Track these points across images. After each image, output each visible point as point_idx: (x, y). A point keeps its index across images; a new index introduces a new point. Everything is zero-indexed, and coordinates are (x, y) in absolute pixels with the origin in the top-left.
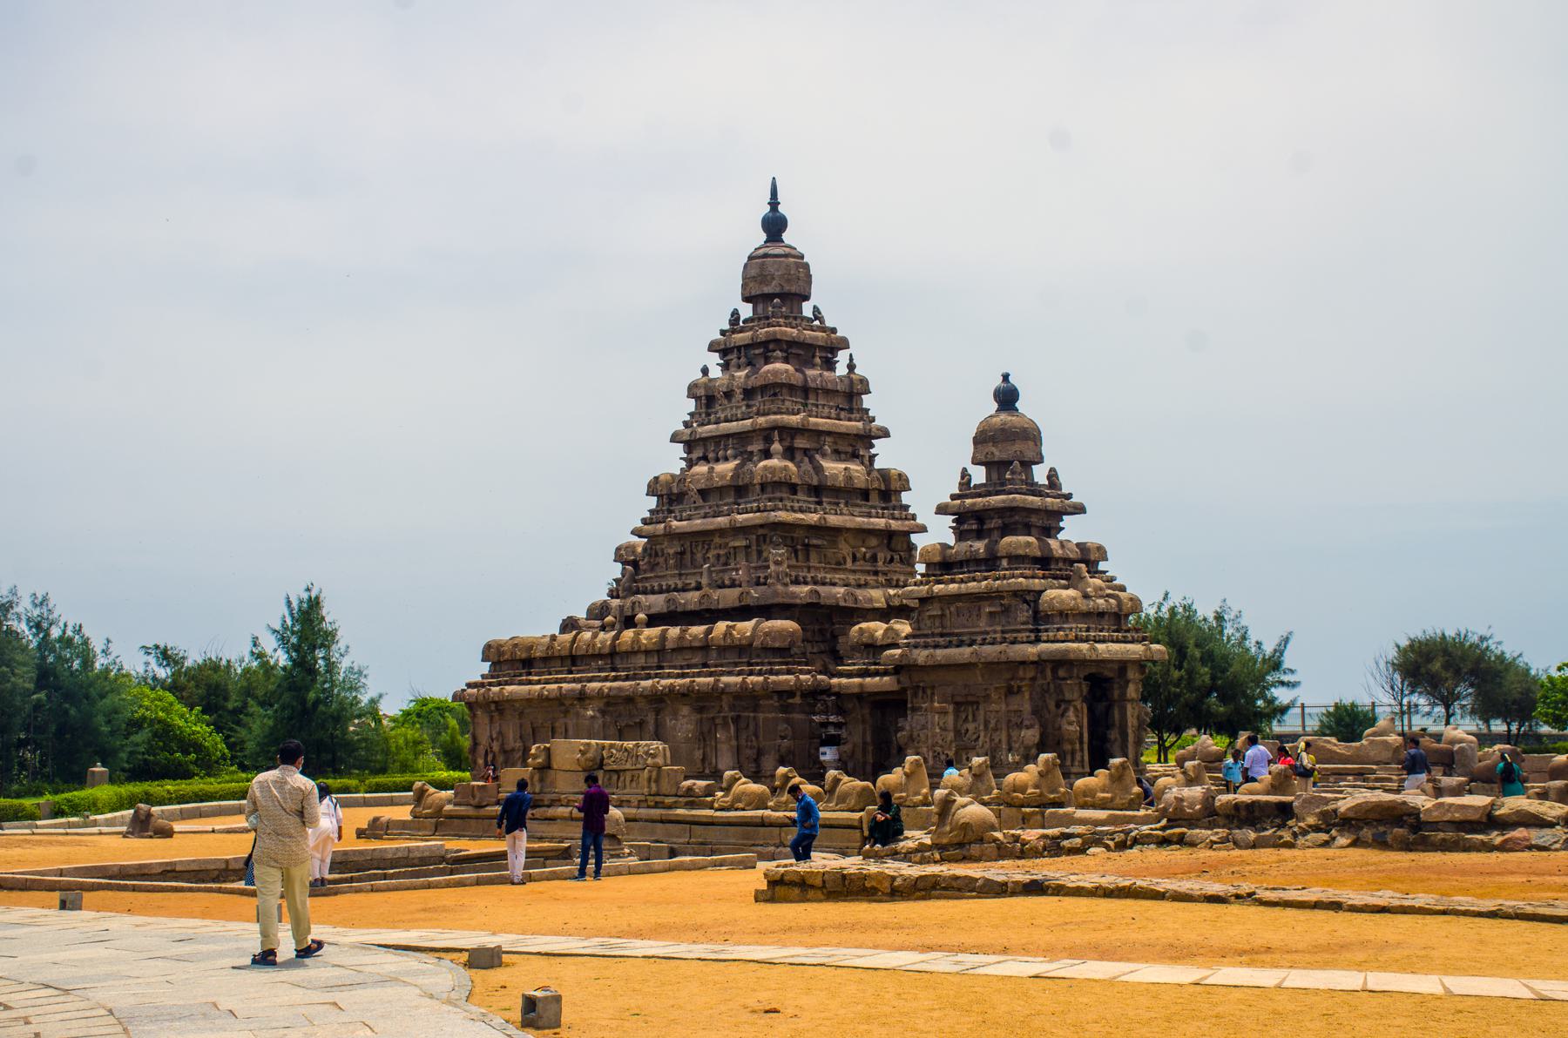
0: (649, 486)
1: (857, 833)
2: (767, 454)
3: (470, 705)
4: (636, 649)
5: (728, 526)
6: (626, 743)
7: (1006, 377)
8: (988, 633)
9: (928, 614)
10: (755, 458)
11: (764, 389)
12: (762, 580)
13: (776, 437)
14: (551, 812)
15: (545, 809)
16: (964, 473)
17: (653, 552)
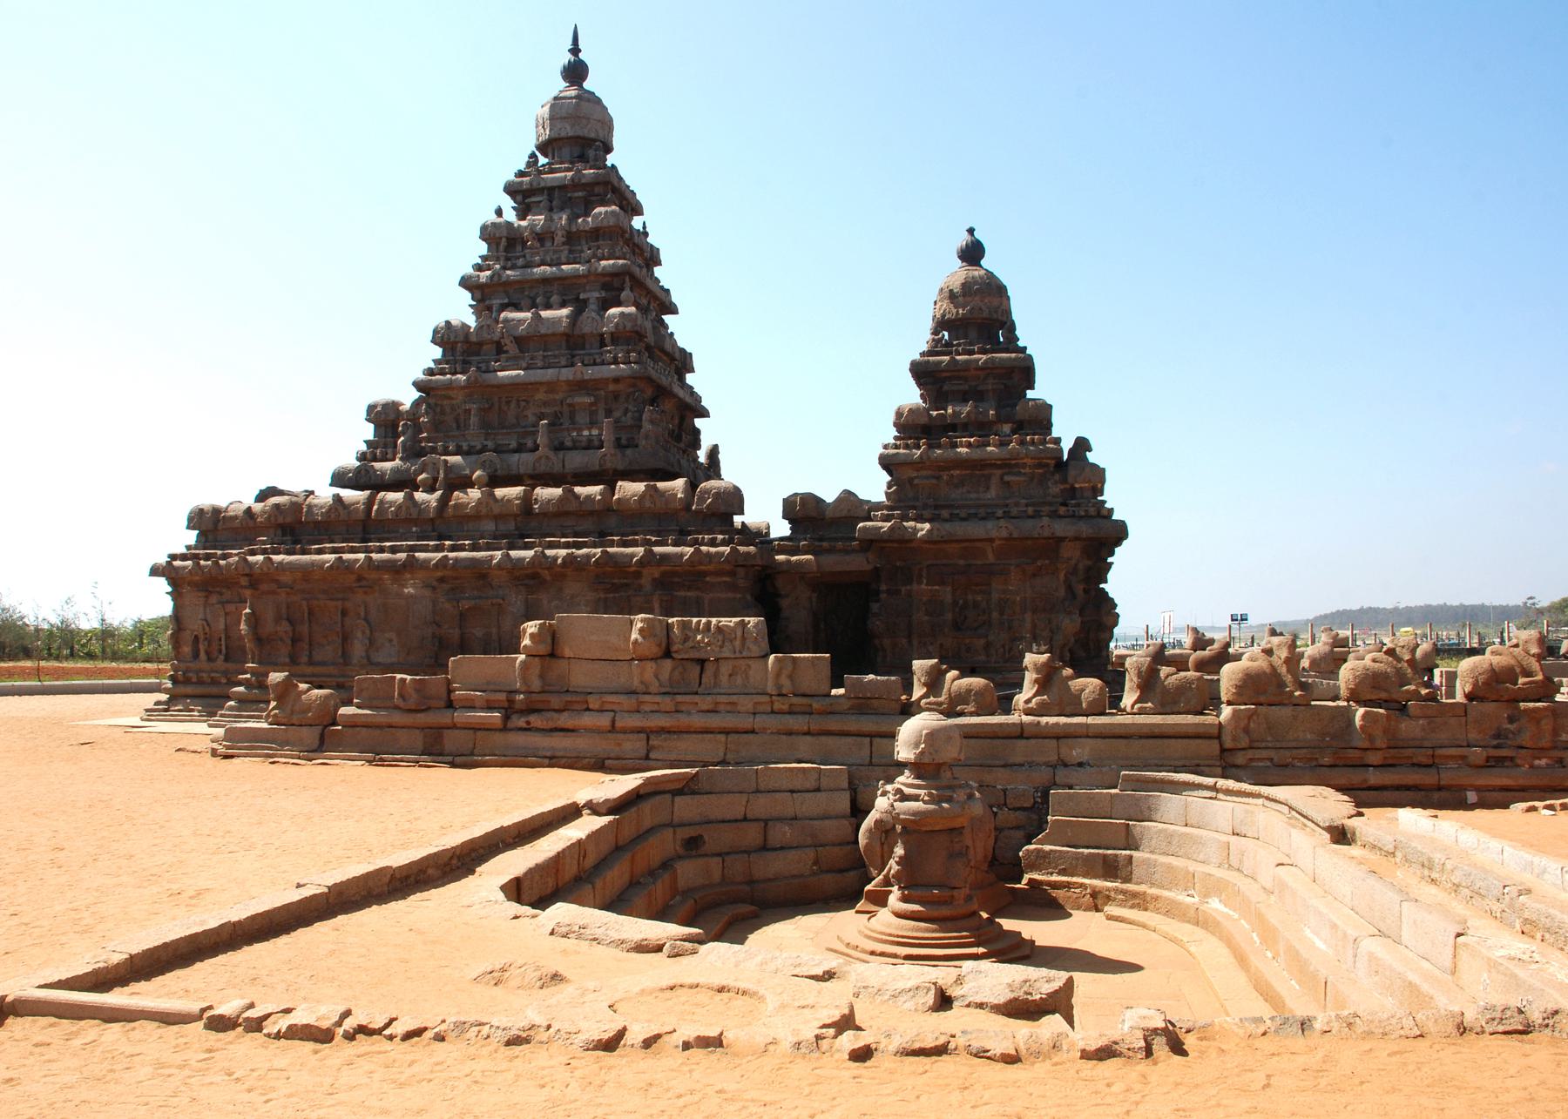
0: (436, 332)
1: (1215, 745)
2: (605, 305)
3: (173, 582)
4: (484, 511)
5: (571, 378)
6: (714, 620)
7: (971, 231)
8: (1007, 506)
9: (916, 481)
10: (593, 306)
11: (596, 234)
12: (624, 442)
13: (628, 284)
14: (565, 720)
15: (553, 714)
16: (935, 332)
17: (438, 410)
